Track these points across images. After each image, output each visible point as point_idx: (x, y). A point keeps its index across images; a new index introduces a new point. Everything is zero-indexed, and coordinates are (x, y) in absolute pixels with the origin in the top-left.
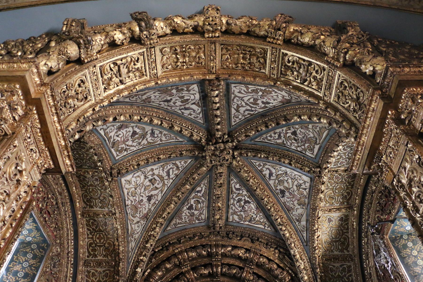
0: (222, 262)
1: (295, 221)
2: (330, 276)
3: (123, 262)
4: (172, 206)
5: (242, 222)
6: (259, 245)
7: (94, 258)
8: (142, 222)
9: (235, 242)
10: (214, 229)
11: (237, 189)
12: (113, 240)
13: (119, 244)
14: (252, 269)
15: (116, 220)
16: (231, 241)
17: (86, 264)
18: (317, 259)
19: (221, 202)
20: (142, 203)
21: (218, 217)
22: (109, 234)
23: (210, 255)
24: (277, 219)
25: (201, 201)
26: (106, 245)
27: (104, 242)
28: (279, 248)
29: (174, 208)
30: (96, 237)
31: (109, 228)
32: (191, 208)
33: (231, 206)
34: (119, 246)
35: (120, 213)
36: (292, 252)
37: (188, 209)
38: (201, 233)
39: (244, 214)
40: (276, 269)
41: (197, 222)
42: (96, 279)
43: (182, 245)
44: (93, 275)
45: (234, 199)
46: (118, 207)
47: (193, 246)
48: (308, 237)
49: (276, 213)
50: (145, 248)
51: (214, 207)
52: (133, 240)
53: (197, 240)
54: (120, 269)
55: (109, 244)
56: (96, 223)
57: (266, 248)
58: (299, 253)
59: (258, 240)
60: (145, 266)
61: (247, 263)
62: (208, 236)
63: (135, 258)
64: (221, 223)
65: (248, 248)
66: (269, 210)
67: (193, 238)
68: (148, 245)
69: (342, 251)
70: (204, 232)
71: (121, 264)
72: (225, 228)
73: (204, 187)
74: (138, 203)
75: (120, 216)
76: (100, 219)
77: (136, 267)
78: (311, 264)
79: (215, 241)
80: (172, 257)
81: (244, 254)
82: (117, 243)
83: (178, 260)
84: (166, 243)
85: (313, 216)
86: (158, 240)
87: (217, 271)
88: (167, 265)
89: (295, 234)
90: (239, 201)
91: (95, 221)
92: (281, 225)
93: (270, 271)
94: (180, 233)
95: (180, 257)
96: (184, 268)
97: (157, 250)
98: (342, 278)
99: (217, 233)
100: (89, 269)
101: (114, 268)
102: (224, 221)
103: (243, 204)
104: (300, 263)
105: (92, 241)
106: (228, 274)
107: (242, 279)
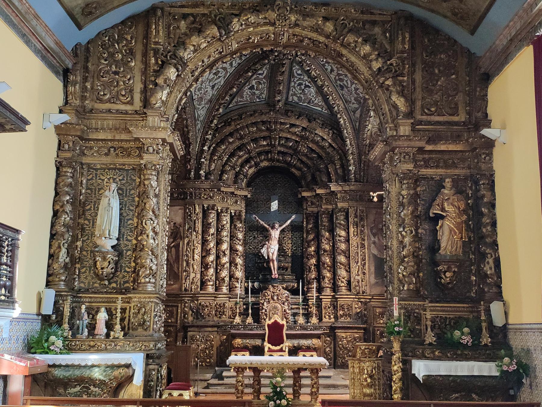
5: (301, 103)
11: (298, 74)
24: (334, 108)
25: (262, 82)
33: (292, 88)
38: (261, 111)
40: (328, 148)
41: (258, 100)
45: (295, 83)
59: (315, 120)
63: (201, 137)
65: (304, 126)
73: (266, 70)
77: (203, 145)
81: (300, 132)
90: (300, 84)
97: (220, 126)
103: (303, 88)
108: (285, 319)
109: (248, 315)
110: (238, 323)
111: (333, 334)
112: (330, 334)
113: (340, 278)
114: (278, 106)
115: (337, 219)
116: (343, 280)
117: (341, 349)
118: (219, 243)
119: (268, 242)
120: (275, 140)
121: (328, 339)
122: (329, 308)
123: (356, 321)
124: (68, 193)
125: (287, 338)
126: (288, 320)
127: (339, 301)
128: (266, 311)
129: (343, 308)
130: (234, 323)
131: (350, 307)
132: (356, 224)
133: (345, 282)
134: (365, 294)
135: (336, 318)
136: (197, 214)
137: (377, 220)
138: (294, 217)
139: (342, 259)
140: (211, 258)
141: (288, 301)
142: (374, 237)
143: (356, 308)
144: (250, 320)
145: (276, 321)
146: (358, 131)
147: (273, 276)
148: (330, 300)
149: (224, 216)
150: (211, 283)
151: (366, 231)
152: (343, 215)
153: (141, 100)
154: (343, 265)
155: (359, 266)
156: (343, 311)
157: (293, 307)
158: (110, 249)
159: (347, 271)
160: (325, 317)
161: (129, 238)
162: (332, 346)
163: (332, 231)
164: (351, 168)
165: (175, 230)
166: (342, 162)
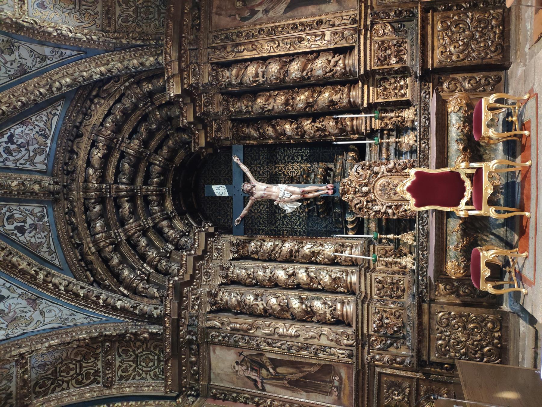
0: (112, 182)
1: (44, 64)
2: (134, 24)
3: (105, 329)
4: (14, 259)
5: (48, 149)
6: (85, 126)
7: (101, 374)
8: (41, 307)
9: (80, 163)
10: (58, 193)
12: (70, 350)
13: (76, 340)
14: (123, 139)
15: (33, 351)
16: (79, 169)
17: (108, 385)
18: (107, 39)
19: (9, 182)
20: (6, 311)
21: (37, 187)
22: (60, 357)
23: (101, 200)
24: (41, 93)
25: (8, 214)
26: (79, 358)
27: (74, 362)
28: (92, 97)
29: (20, 257)
30: (65, 377)
31: (48, 359)
32: (21, 229)
33: (18, 164)
34: (79, 340)
35: (20, 347)
36: (96, 77)
37: (23, 234)
38: (66, 214)
39: (33, 145)
40: (124, 104)
41: (46, 219)
42: (131, 366)
43: (84, 242)
44: (125, 370)
46: (7, 352)
47: (85, 225)
48: (71, 48)
49: (29, 94)
50: (86, 298)
51: (19, 193)
52: (73, 317)
53: (76, 219)
54: (115, 334)
55: (76, 355)
56: (41, 381)
57: (91, 116)
58: (97, 66)
59: (78, 128)
60: (114, 295)
61: (113, 145)
62: (71, 202)
63: (101, 311)
64: (47, 182)
65: (90, 144)
66: (24, 104)
67: (74, 225)
68: (82, 293)
70: (64, 209)
71: (107, 333)
72: (57, 175)
74: (6, 318)
75: (26, 345)
76: (34, 376)
77: (114, 308)
78: (114, 51)
79: (78, 192)
80: (102, 255)
81: (100, 150)
82: (75, 342)
83: (107, 246)
84: (80, 266)
85: (31, 31)
86: (75, 278)
87: (126, 191)
88: (114, 263)
89: (67, 68)
91: (36, 384)
92: (51, 87)
93: (126, 115)
94: (66, 245)
95: (102, 244)
96: (121, 238)
97: (92, 279)
98: (137, 7)
99: (65, 190)
100: (117, 378)
101: (115, 342)
102: (45, 178)
104: (113, 67)
105: (73, 381)
106: (130, 175)
107: (138, 155)
108: (406, 171)
109: (398, 240)
110: (414, 259)
111: (437, 76)
112: (436, 81)
113: (328, 70)
114: (51, 187)
116: (332, 63)
118: (274, 284)
119: (274, 201)
120: (122, 190)
121: (445, 85)
122: (385, 89)
123: (409, 32)
125: (446, 166)
126: (408, 165)
127: (371, 67)
128: (390, 207)
129: (385, 59)
130: (414, 267)
131: (383, 47)
133: (336, 59)
134: (358, 18)
135: (404, 72)
136: (222, 324)
137: (229, 12)
139: (295, 68)
140: (295, 304)
141: (370, 166)
142: (256, 12)
143: (384, 34)
144: (408, 238)
145: (409, 189)
147: (331, 192)
148: (371, 88)
149: (233, 273)
150: (339, 306)
152: (222, 71)
155: (308, 34)
156: (390, 58)
157: (384, 156)
160: (403, 96)
162: (459, 76)
164: (148, 64)
165: (248, 364)
166: (144, 80)
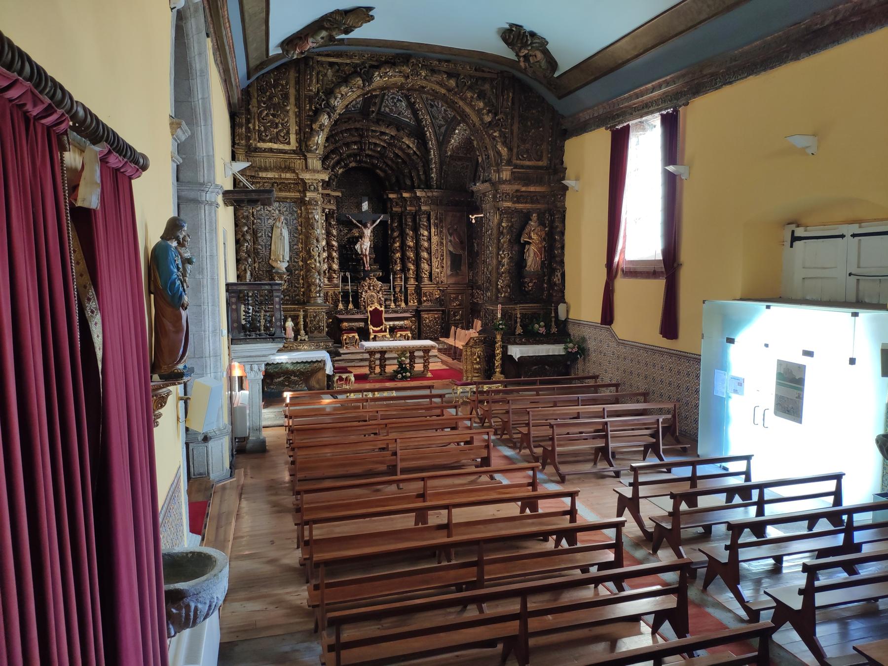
69: (466, 154)
93: (408, 155)
115: (420, 220)
117: (425, 327)
121: (414, 319)
122: (413, 294)
124: (245, 224)
131: (431, 294)
132: (436, 226)
133: (428, 274)
135: (420, 302)
138: (382, 216)
139: (425, 255)
145: (376, 308)
146: (442, 143)
151: (444, 231)
153: (297, 141)
154: (426, 260)
158: (285, 270)
159: (428, 265)
161: (296, 260)
162: (417, 324)
163: (416, 229)
